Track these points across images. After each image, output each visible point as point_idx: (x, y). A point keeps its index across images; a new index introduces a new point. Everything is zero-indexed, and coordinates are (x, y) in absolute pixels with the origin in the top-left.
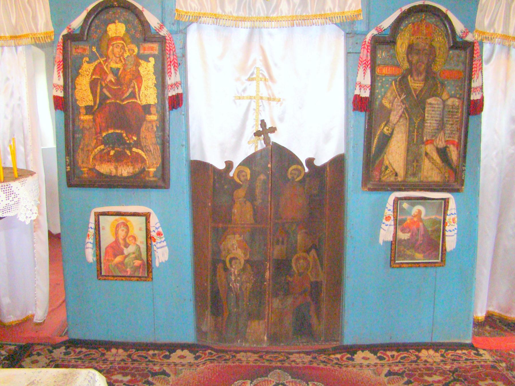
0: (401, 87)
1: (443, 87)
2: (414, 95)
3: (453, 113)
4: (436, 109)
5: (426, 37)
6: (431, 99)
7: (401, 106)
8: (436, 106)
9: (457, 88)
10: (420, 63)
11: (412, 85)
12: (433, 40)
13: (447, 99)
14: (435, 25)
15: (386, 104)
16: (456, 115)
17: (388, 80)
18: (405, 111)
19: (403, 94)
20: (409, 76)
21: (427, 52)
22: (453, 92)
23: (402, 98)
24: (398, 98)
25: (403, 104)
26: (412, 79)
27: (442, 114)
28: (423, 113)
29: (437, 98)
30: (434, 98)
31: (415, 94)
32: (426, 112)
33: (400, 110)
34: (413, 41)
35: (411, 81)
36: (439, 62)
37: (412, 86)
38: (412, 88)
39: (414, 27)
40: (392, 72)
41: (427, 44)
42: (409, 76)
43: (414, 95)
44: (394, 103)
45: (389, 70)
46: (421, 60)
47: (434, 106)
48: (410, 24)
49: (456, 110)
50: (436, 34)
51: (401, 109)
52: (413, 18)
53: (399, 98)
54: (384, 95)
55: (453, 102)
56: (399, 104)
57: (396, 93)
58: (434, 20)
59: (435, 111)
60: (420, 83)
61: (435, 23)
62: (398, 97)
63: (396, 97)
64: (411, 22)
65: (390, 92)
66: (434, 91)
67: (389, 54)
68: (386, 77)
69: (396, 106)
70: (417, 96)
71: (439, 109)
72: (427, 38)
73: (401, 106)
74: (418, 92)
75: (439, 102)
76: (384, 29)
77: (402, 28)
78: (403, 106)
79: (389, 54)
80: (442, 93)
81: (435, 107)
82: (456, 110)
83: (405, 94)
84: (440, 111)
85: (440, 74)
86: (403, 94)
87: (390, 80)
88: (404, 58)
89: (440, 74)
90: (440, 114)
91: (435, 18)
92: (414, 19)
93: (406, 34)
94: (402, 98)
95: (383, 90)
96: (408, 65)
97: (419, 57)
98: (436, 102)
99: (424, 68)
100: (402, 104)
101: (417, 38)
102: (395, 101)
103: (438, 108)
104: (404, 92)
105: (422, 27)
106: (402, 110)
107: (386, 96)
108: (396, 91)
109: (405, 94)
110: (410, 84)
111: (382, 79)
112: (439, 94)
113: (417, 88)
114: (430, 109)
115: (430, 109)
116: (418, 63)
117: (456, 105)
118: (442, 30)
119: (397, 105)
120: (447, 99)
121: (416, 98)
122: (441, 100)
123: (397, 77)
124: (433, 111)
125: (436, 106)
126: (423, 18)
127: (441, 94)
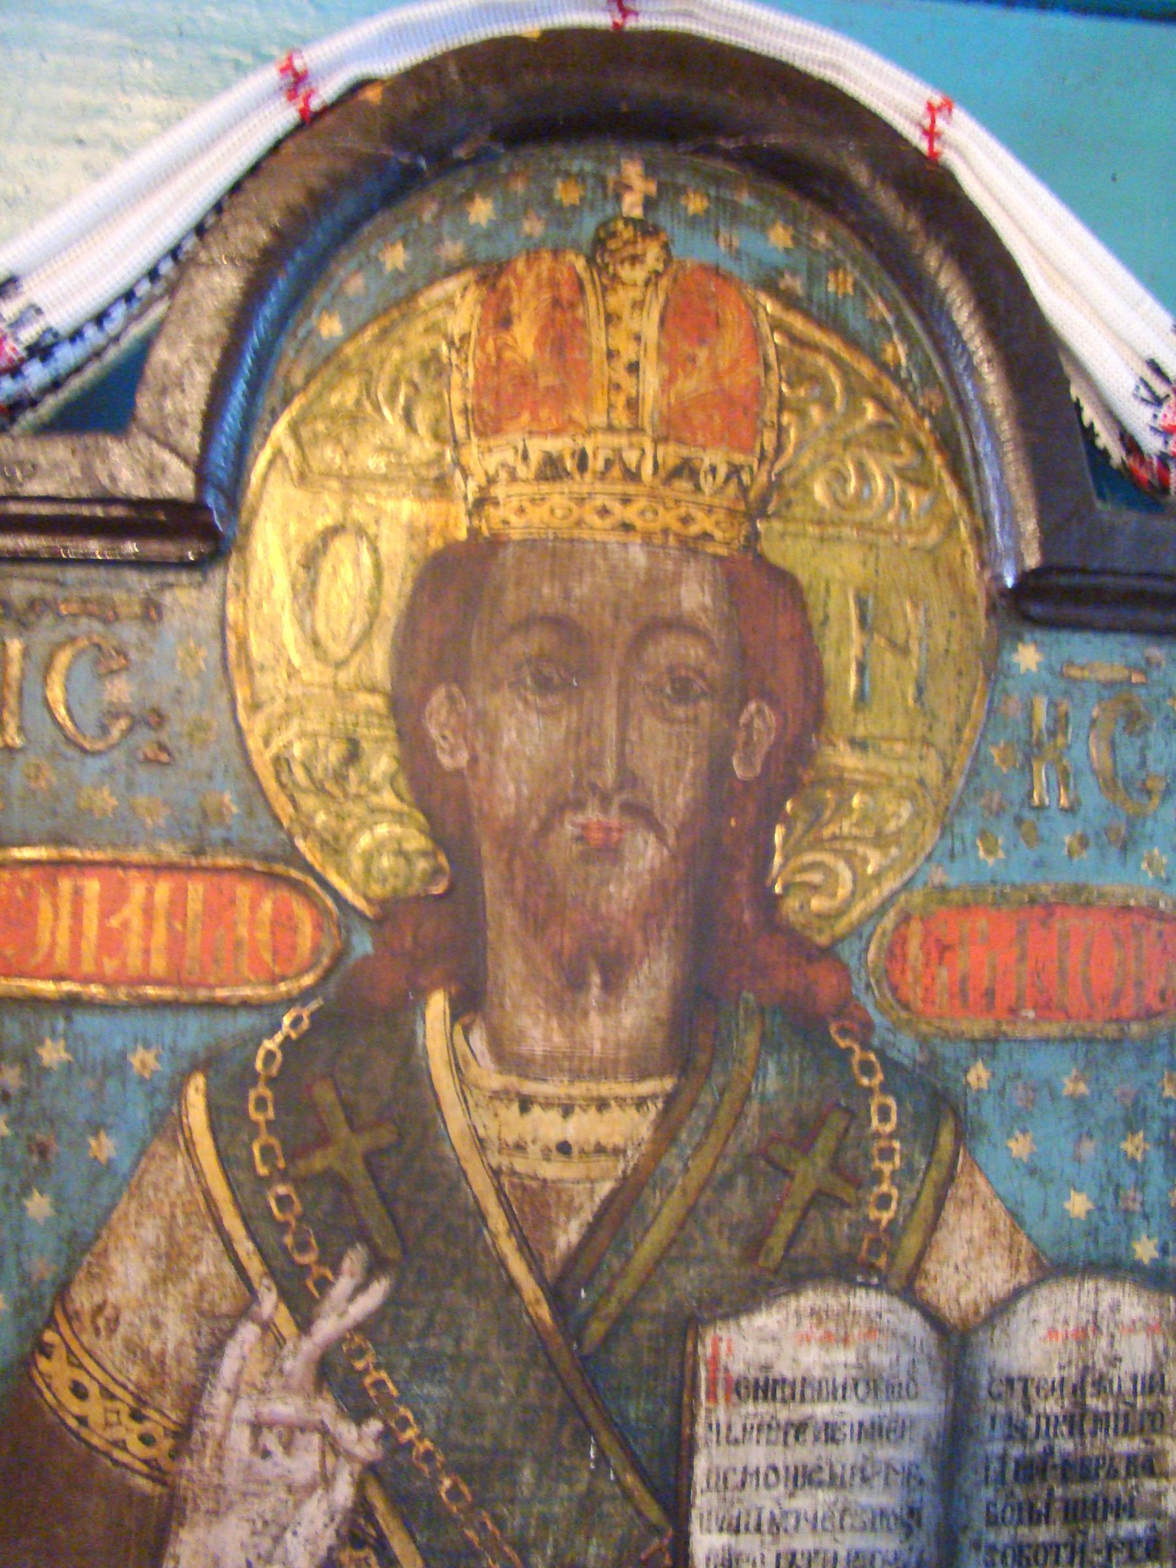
0: (319, 1162)
1: (946, 1139)
2: (518, 1268)
3: (1092, 1489)
4: (848, 1453)
5: (671, 454)
6: (766, 1320)
7: (331, 1444)
8: (852, 1411)
9: (1133, 1146)
10: (592, 814)
11: (488, 1127)
12: (776, 485)
13: (1002, 1307)
14: (789, 301)
15: (94, 1409)
16: (1125, 1509)
17: (118, 1066)
18: (379, 1503)
19: (354, 1261)
20: (437, 1004)
21: (694, 652)
22: (1078, 1204)
23: (327, 1327)
24: (267, 1326)
25: (359, 1416)
26: (478, 1040)
27: (929, 1514)
28: (654, 1513)
29: (866, 1301)
30: (810, 1299)
31: (534, 1263)
32: (703, 1501)
33: (299, 1493)
34: (482, 501)
35: (458, 1068)
36: (867, 788)
37: (481, 1144)
38: (481, 1185)
39: (505, 322)
40: (176, 943)
41: (691, 547)
42: (437, 1004)
43: (518, 1268)
44: (220, 1399)
45: (132, 912)
46: (609, 775)
47: (822, 1411)
48: (452, 286)
49: (1125, 1446)
50: (815, 413)
51: (326, 1480)
52: (482, 211)
53: (285, 1322)
54: (63, 1290)
55: (1081, 1337)
56: (286, 1408)
57: (244, 1247)
58: (780, 236)
59: (836, 1482)
60: (602, 1104)
61: (797, 285)
62: (269, 1301)
63: (245, 1310)
64: (452, 250)
65: (151, 1230)
66: (822, 1199)
67: (121, 690)
68: (87, 1023)
69: (241, 1438)
70: (556, 1294)
71: (885, 1452)
72: (686, 470)
73: (331, 1444)
74: (568, 1235)
75: (881, 1358)
76: (28, 334)
77: (331, 327)
78: (347, 1432)
79: (121, 690)
80: (934, 1225)
81: (830, 1433)
82: (1125, 1446)
83: (374, 1268)
84: (910, 1476)
85: (895, 951)
86: (354, 1261)
87: (142, 1060)
88: (353, 755)
89: (895, 951)
90: (910, 1519)
91: (793, 221)
92: (508, 216)
93: (392, 418)
94: (327, 1327)
95: (38, 1205)
96: (416, 841)
97: (577, 736)
98: (844, 1357)
99: (661, 887)
100: (326, 1409)
101: (552, 470)
102: (229, 1366)
103: (871, 1432)
104: (362, 1235)
105: (610, 319)
106: (344, 1492)
107: (83, 1298)
108: (233, 1224)
109: (374, 1268)
110: (455, 1120)
111: (27, 1059)
112: (894, 1231)
113: (550, 1170)
114: (757, 1455)
115: (757, 1455)
116: (560, 808)
117: (1121, 1375)
118: (891, 371)
119: (257, 1427)
120: (1002, 1307)
121: (544, 1312)
122: (912, 1322)
123: (244, 1021)
124: (803, 1478)
125: (852, 1411)
126: (631, 205)
127: (911, 1243)
